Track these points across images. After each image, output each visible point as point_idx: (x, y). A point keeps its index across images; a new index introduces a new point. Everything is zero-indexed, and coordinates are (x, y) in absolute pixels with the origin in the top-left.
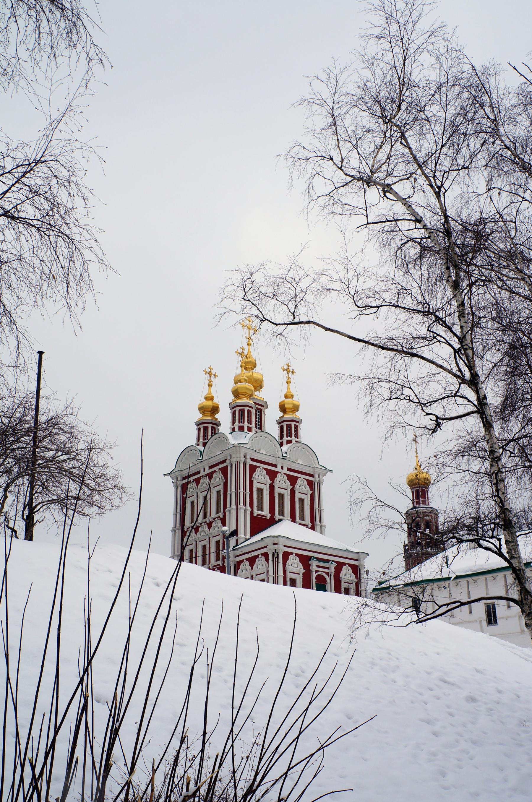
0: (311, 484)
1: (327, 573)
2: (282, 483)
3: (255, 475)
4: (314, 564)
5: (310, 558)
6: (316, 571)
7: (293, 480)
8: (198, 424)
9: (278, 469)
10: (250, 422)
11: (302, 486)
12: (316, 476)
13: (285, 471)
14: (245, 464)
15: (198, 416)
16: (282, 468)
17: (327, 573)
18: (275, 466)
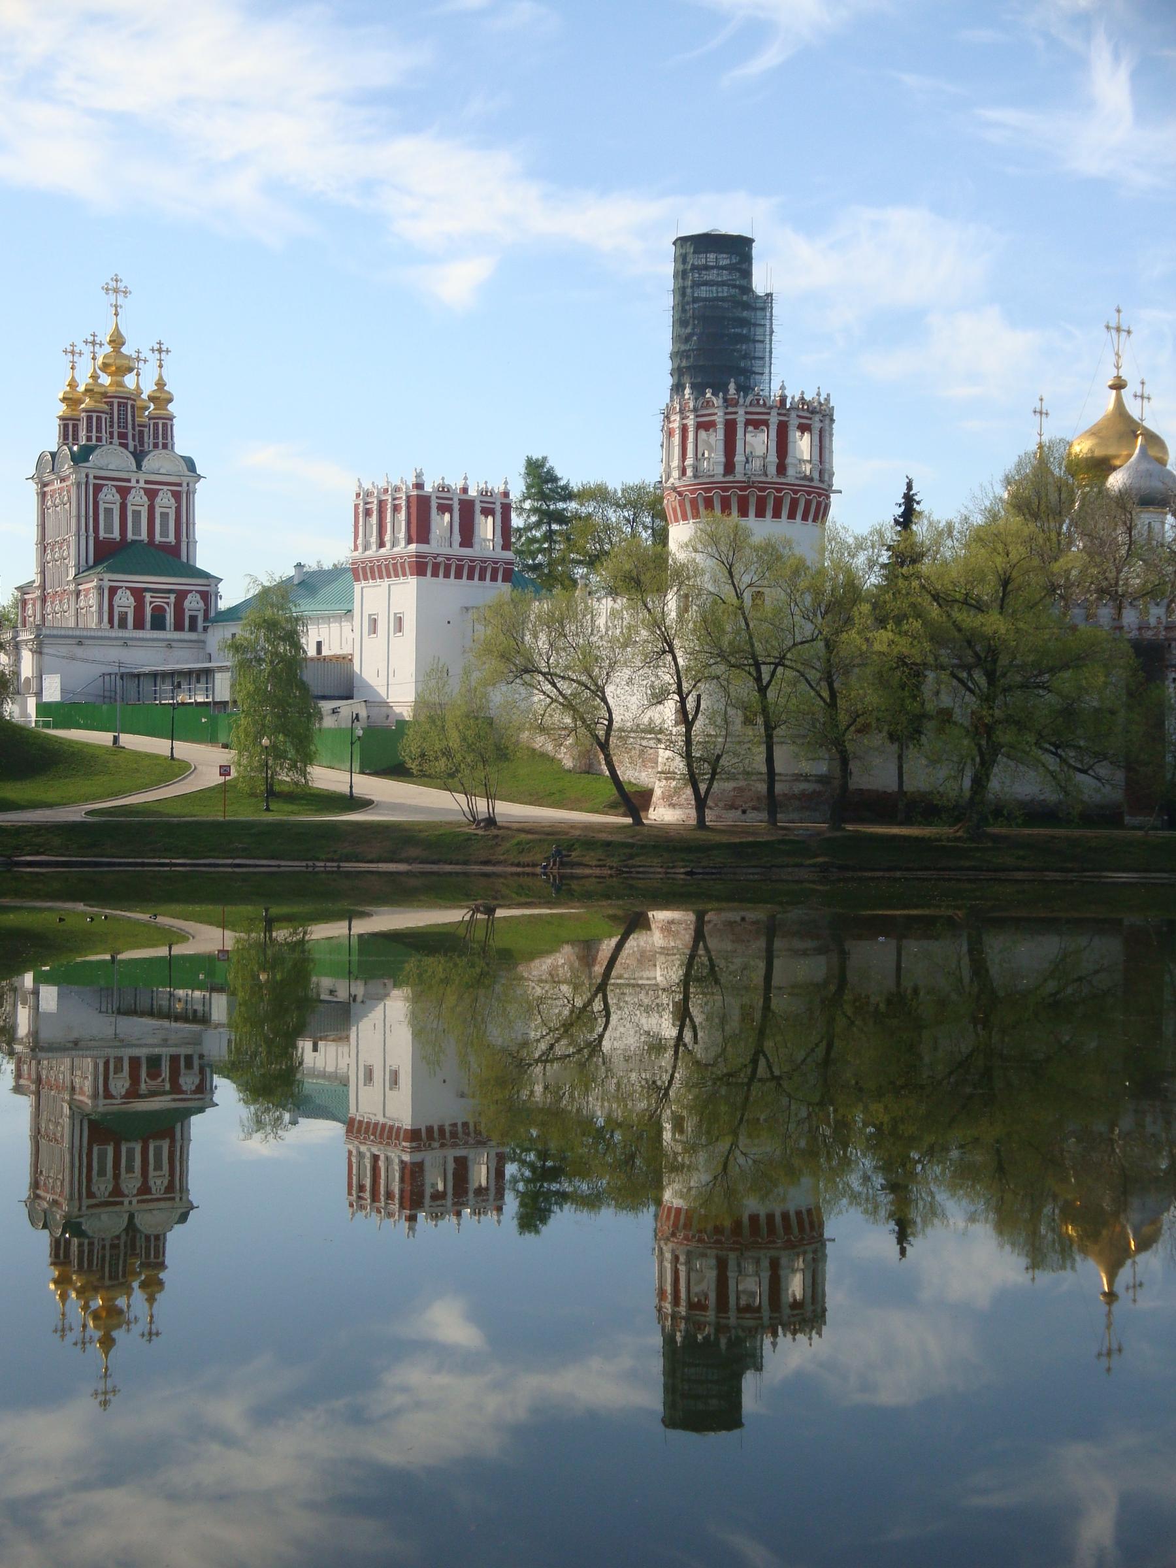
0: (177, 496)
1: (167, 603)
2: (138, 499)
3: (101, 496)
4: (148, 596)
5: (146, 590)
6: (151, 603)
7: (151, 495)
8: (62, 418)
9: (134, 483)
10: (99, 430)
11: (165, 500)
12: (185, 485)
13: (142, 484)
14: (87, 483)
15: (61, 409)
16: (138, 482)
17: (167, 603)
18: (129, 481)
